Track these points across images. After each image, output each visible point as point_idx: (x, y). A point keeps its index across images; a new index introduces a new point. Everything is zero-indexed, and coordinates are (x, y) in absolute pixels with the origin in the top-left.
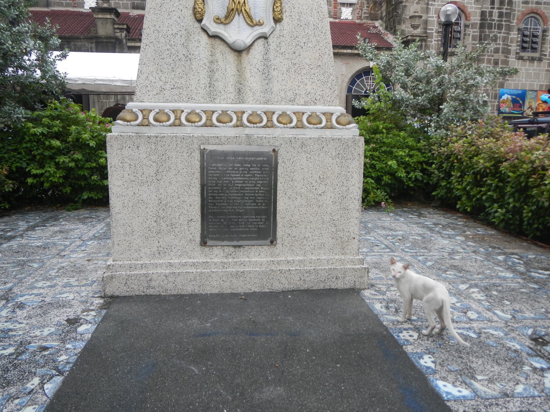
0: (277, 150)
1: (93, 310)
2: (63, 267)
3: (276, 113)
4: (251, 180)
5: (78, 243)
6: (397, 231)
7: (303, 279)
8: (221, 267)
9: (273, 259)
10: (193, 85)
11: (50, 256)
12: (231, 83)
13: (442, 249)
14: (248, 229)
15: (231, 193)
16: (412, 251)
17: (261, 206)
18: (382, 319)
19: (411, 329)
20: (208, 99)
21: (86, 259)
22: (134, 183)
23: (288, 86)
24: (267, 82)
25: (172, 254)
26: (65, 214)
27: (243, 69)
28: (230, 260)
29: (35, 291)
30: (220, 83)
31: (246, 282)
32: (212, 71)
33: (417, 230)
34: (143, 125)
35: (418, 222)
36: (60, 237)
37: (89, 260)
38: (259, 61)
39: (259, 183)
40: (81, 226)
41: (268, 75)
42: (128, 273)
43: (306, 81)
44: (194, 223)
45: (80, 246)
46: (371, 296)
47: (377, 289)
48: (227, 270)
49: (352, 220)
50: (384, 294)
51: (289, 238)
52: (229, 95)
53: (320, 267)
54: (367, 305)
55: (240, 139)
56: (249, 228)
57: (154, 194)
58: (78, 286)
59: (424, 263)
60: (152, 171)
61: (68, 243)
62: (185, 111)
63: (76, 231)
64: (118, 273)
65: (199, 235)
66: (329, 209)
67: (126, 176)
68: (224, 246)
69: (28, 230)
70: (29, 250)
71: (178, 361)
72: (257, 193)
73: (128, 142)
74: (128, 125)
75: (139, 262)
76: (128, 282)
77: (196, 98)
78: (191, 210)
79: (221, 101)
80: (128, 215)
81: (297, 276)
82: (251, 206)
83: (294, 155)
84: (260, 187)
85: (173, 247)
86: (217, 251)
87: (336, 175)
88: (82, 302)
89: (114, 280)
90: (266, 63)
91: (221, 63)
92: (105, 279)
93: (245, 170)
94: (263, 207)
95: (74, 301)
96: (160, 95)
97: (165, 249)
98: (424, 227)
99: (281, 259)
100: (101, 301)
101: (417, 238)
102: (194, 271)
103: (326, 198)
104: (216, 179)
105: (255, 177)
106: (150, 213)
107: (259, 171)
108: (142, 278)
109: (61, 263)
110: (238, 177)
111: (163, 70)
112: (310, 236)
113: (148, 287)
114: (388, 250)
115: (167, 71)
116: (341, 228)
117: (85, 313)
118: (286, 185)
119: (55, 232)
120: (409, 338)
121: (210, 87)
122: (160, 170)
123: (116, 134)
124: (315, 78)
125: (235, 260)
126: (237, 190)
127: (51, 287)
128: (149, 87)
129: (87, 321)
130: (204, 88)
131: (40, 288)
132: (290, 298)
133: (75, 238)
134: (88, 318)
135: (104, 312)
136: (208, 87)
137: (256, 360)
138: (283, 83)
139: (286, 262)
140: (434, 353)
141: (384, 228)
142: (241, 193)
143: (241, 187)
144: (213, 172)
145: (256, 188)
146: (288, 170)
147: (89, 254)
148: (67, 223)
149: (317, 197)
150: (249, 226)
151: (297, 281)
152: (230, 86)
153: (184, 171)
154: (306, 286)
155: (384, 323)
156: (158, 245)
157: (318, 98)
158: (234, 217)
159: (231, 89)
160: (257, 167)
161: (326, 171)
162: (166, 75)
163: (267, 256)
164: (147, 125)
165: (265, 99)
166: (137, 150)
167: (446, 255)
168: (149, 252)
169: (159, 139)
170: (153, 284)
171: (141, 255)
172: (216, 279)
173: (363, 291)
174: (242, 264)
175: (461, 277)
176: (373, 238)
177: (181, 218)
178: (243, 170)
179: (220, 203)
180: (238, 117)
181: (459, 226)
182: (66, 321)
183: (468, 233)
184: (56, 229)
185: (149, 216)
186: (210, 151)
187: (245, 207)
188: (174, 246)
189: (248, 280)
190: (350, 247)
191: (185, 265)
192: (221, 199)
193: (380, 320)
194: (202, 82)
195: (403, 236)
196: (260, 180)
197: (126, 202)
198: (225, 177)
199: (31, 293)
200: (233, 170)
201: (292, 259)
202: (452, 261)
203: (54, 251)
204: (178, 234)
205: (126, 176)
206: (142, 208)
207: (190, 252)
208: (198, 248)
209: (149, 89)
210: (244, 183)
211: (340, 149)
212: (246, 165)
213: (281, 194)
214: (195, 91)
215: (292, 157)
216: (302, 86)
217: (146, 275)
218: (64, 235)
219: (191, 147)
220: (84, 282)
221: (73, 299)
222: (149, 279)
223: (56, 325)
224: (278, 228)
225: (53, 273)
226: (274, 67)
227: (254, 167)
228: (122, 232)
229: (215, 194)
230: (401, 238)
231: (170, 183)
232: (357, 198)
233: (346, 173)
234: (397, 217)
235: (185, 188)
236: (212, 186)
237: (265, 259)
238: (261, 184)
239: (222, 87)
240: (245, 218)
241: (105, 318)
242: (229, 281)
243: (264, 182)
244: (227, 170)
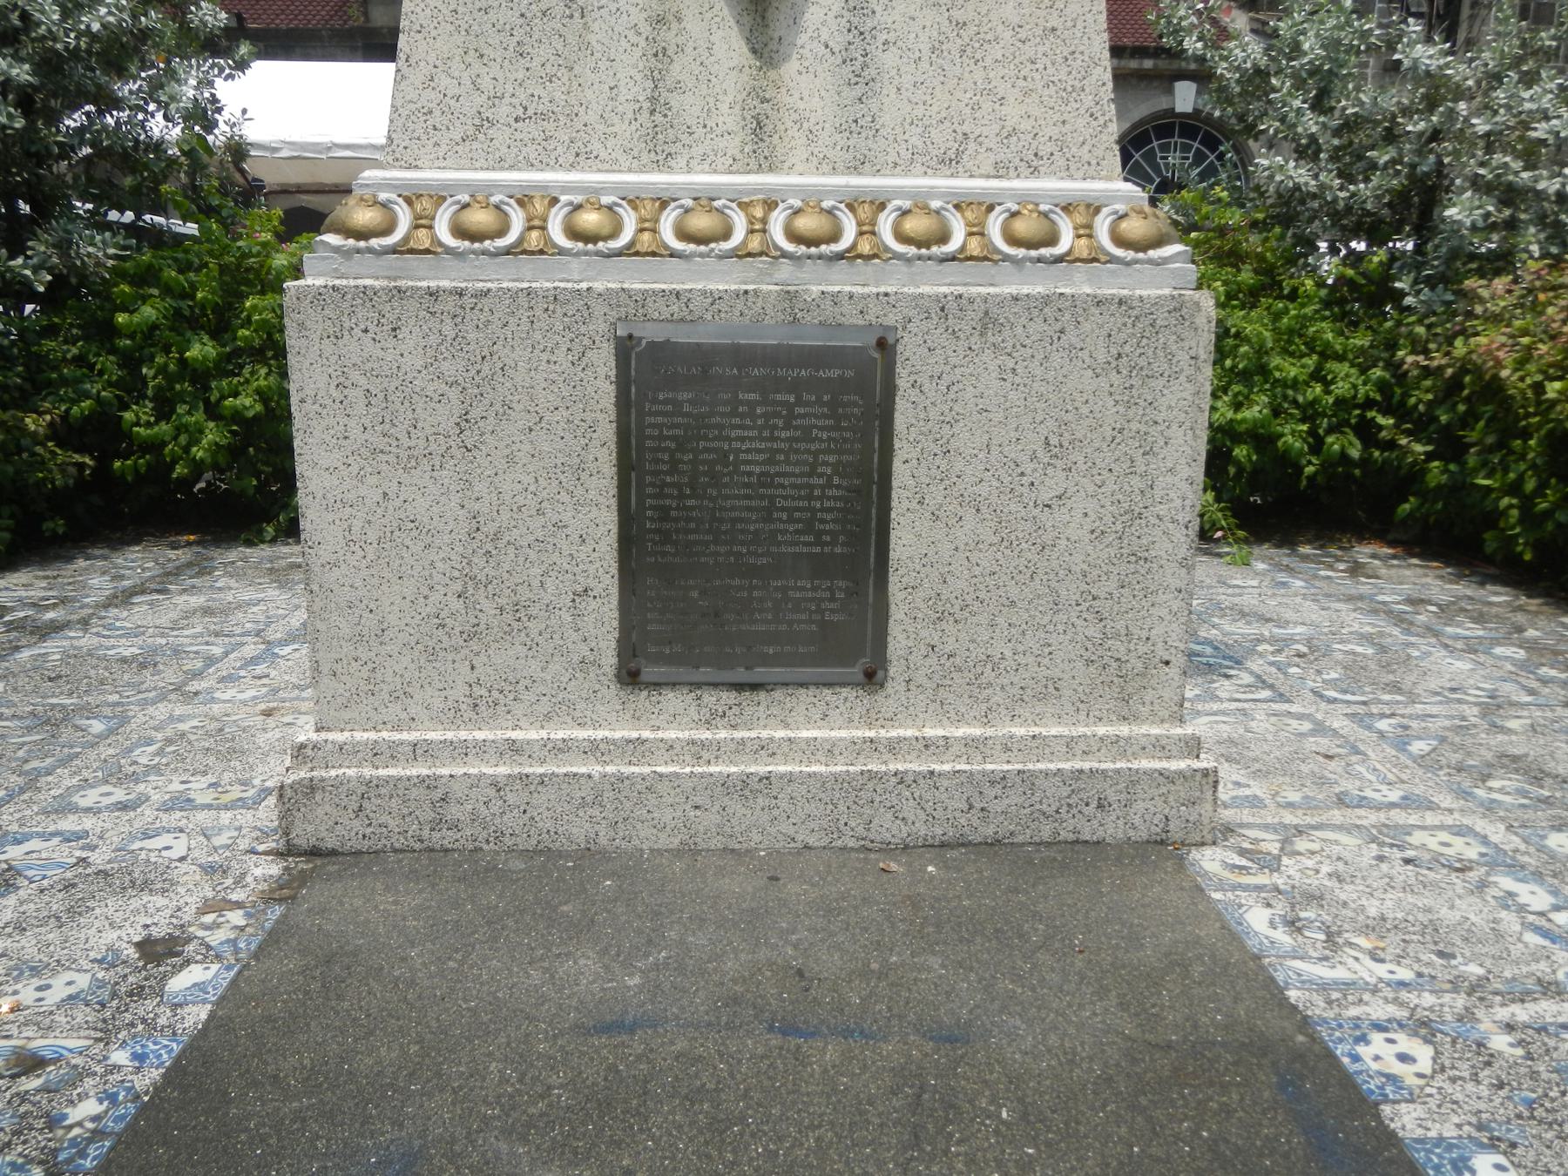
0: (891, 341)
1: (238, 905)
2: (183, 735)
3: (890, 207)
4: (797, 451)
5: (250, 650)
6: (1288, 622)
7: (978, 806)
8: (688, 758)
9: (872, 734)
10: (594, 106)
11: (153, 694)
12: (730, 98)
13: (1453, 690)
14: (784, 627)
15: (727, 497)
16: (1349, 697)
17: (833, 543)
18: (1280, 977)
19: (1401, 1026)
20: (645, 158)
21: (263, 706)
22: (384, 458)
23: (935, 108)
24: (858, 90)
25: (519, 709)
26: (234, 554)
27: (773, 45)
28: (722, 734)
29: (68, 824)
30: (689, 98)
31: (776, 812)
32: (661, 54)
33: (1356, 621)
34: (412, 251)
35: (1353, 591)
36: (199, 629)
37: (268, 713)
38: (831, 14)
39: (826, 464)
40: (272, 592)
41: (865, 66)
42: (368, 772)
43: (1002, 88)
44: (593, 604)
45: (254, 661)
46: (1226, 874)
47: (1246, 845)
48: (713, 769)
49: (1161, 598)
50: (1272, 864)
51: (933, 660)
52: (721, 143)
53: (1040, 766)
54: (1219, 914)
55: (760, 303)
56: (790, 623)
57: (456, 499)
58: (209, 807)
59: (1401, 744)
60: (445, 416)
61: (217, 651)
62: (564, 198)
63: (255, 609)
64: (333, 773)
65: (614, 644)
66: (1078, 558)
67: (355, 431)
68: (698, 685)
69: (107, 605)
70: (92, 673)
71: (504, 1147)
72: (820, 498)
73: (361, 313)
74: (358, 251)
75: (405, 736)
76: (366, 804)
77: (603, 155)
78: (583, 556)
79: (693, 163)
80: (365, 573)
81: (957, 795)
82: (797, 544)
83: (953, 361)
84: (830, 478)
85: (520, 687)
86: (673, 700)
87: (1109, 433)
88: (209, 870)
89: (318, 797)
90: (855, 21)
91: (692, 24)
92: (289, 793)
93: (777, 415)
94: (838, 550)
95: (184, 867)
96: (475, 145)
97: (495, 694)
98: (1375, 612)
99: (902, 732)
100: (274, 869)
101: (1359, 649)
102: (596, 769)
103: (1068, 518)
104: (673, 445)
105: (813, 440)
106: (439, 565)
107: (825, 416)
108: (414, 793)
109: (181, 719)
110: (751, 439)
111: (487, 51)
112: (1008, 653)
113: (436, 825)
114: (1266, 694)
115: (498, 55)
116: (1121, 625)
117: (209, 918)
118: (923, 470)
119: (189, 614)
120: (1398, 1068)
121: (652, 112)
122: (473, 415)
123: (320, 282)
124: (1037, 76)
125: (738, 734)
126: (747, 485)
127: (123, 807)
128: (437, 113)
129: (209, 948)
130: (630, 115)
131: (88, 810)
132: (932, 877)
133: (243, 635)
134: (216, 938)
135: (277, 911)
136: (646, 114)
137: (801, 1153)
138: (919, 95)
139: (920, 746)
140: (1514, 1145)
141: (1243, 614)
142: (762, 497)
143: (762, 474)
144: (660, 420)
145: (815, 481)
146: (933, 414)
147: (275, 691)
148: (233, 583)
149: (1036, 512)
150: (790, 616)
151: (958, 814)
152: (724, 108)
153: (557, 416)
154: (990, 831)
155: (1293, 995)
156: (472, 678)
157: (1045, 150)
158: (737, 582)
159: (729, 120)
160: (819, 402)
161: (1069, 417)
162: (495, 70)
163: (851, 720)
164: (427, 251)
165: (849, 156)
166: (391, 342)
167: (1472, 712)
168: (437, 703)
169: (468, 301)
170: (454, 812)
171: (413, 711)
172: (670, 800)
173: (1195, 854)
174: (765, 749)
175: (1546, 801)
176: (1209, 650)
177: (549, 583)
178: (764, 415)
179: (688, 531)
180: (751, 220)
181: (1494, 610)
182: (139, 945)
183: (1531, 633)
184: (196, 601)
185: (438, 577)
186: (652, 344)
187: (774, 549)
188: (523, 683)
189: (784, 804)
190: (1149, 695)
191: (561, 749)
192: (689, 520)
193: (1273, 980)
194: (624, 94)
195: (1309, 642)
196: (828, 451)
197: (357, 525)
198: (706, 438)
199: (52, 828)
200: (734, 414)
201: (940, 732)
202: (1500, 737)
203: (170, 676)
204: (540, 639)
205: (355, 431)
206: (414, 549)
207: (581, 705)
208: (612, 691)
209: (437, 118)
210: (771, 461)
211: (1123, 336)
212: (779, 397)
213: (906, 504)
214: (601, 128)
215: (948, 368)
216: (987, 106)
217: (428, 783)
218: (212, 623)
219: (583, 329)
220: (236, 792)
221: (182, 859)
222: (438, 794)
223: (99, 962)
224: (891, 621)
225: (144, 756)
226: (882, 37)
227: (808, 404)
228: (346, 630)
229: (668, 502)
230: (1304, 649)
231: (510, 460)
232: (1183, 517)
233: (1143, 428)
234: (1282, 577)
235: (562, 477)
236: (656, 473)
237: (843, 734)
238: (835, 466)
239: (696, 111)
240: (777, 589)
241: (274, 939)
242: (717, 807)
243: (845, 458)
244: (712, 414)
